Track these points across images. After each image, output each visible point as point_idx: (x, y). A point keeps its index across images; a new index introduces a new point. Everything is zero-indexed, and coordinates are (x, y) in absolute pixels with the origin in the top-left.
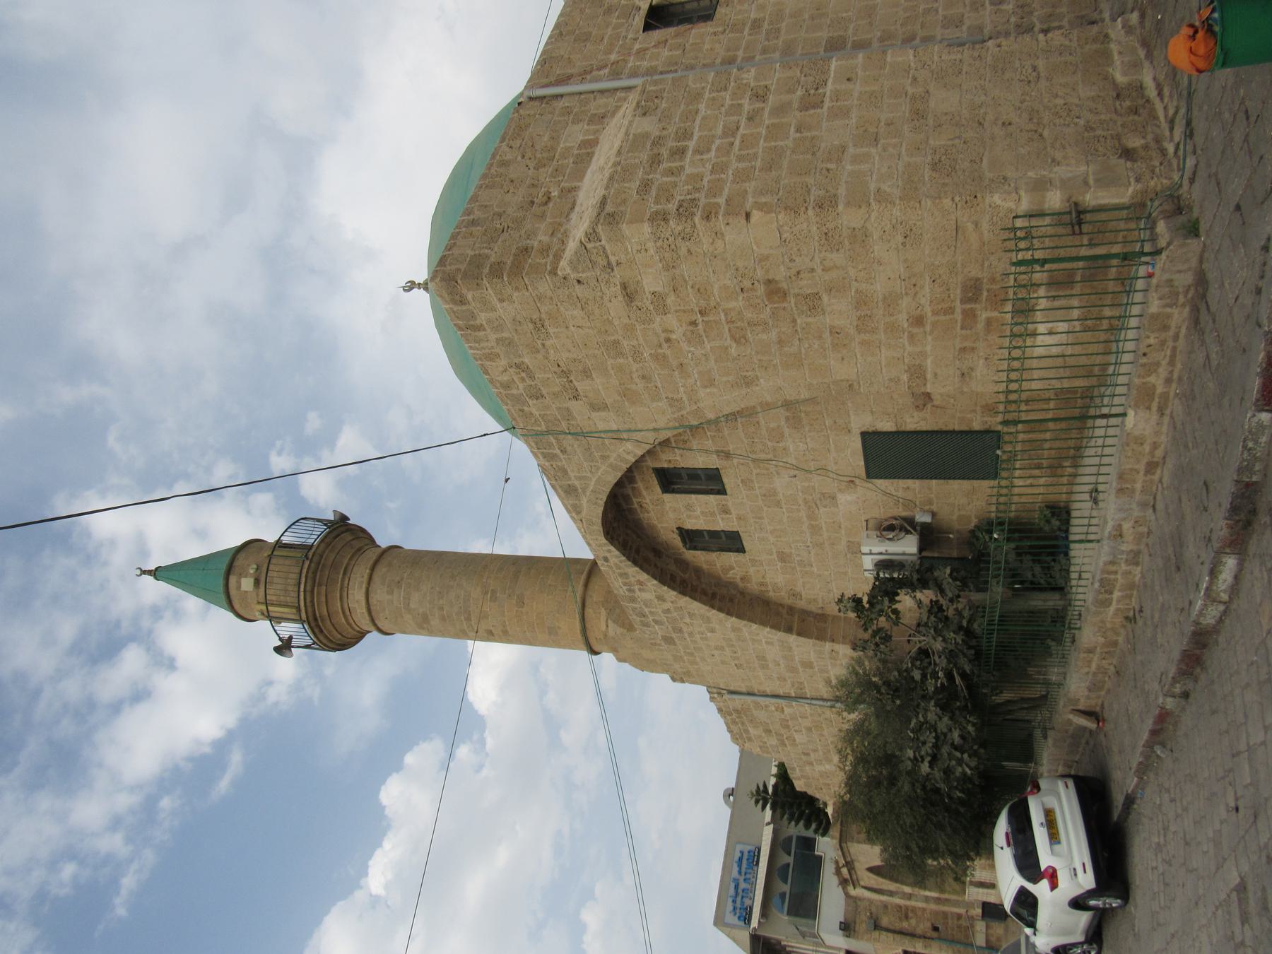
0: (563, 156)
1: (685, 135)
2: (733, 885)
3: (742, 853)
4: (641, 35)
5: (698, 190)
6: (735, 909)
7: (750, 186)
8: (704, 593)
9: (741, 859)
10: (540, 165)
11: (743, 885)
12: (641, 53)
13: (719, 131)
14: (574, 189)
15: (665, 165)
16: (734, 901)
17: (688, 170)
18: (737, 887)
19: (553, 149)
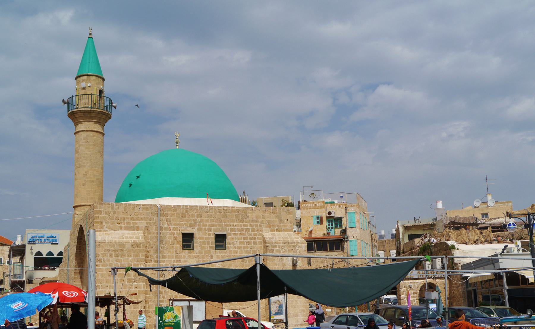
0: (134, 223)
1: (122, 256)
2: (42, 235)
3: (55, 237)
4: (180, 232)
5: (105, 262)
6: (34, 237)
7: (104, 272)
8: (80, 247)
9: (53, 237)
10: (131, 218)
11: (43, 239)
12: (173, 234)
13: (123, 263)
14: (121, 228)
15: (113, 253)
16: (36, 237)
17: (111, 259)
18: (42, 237)
19: (137, 219)
